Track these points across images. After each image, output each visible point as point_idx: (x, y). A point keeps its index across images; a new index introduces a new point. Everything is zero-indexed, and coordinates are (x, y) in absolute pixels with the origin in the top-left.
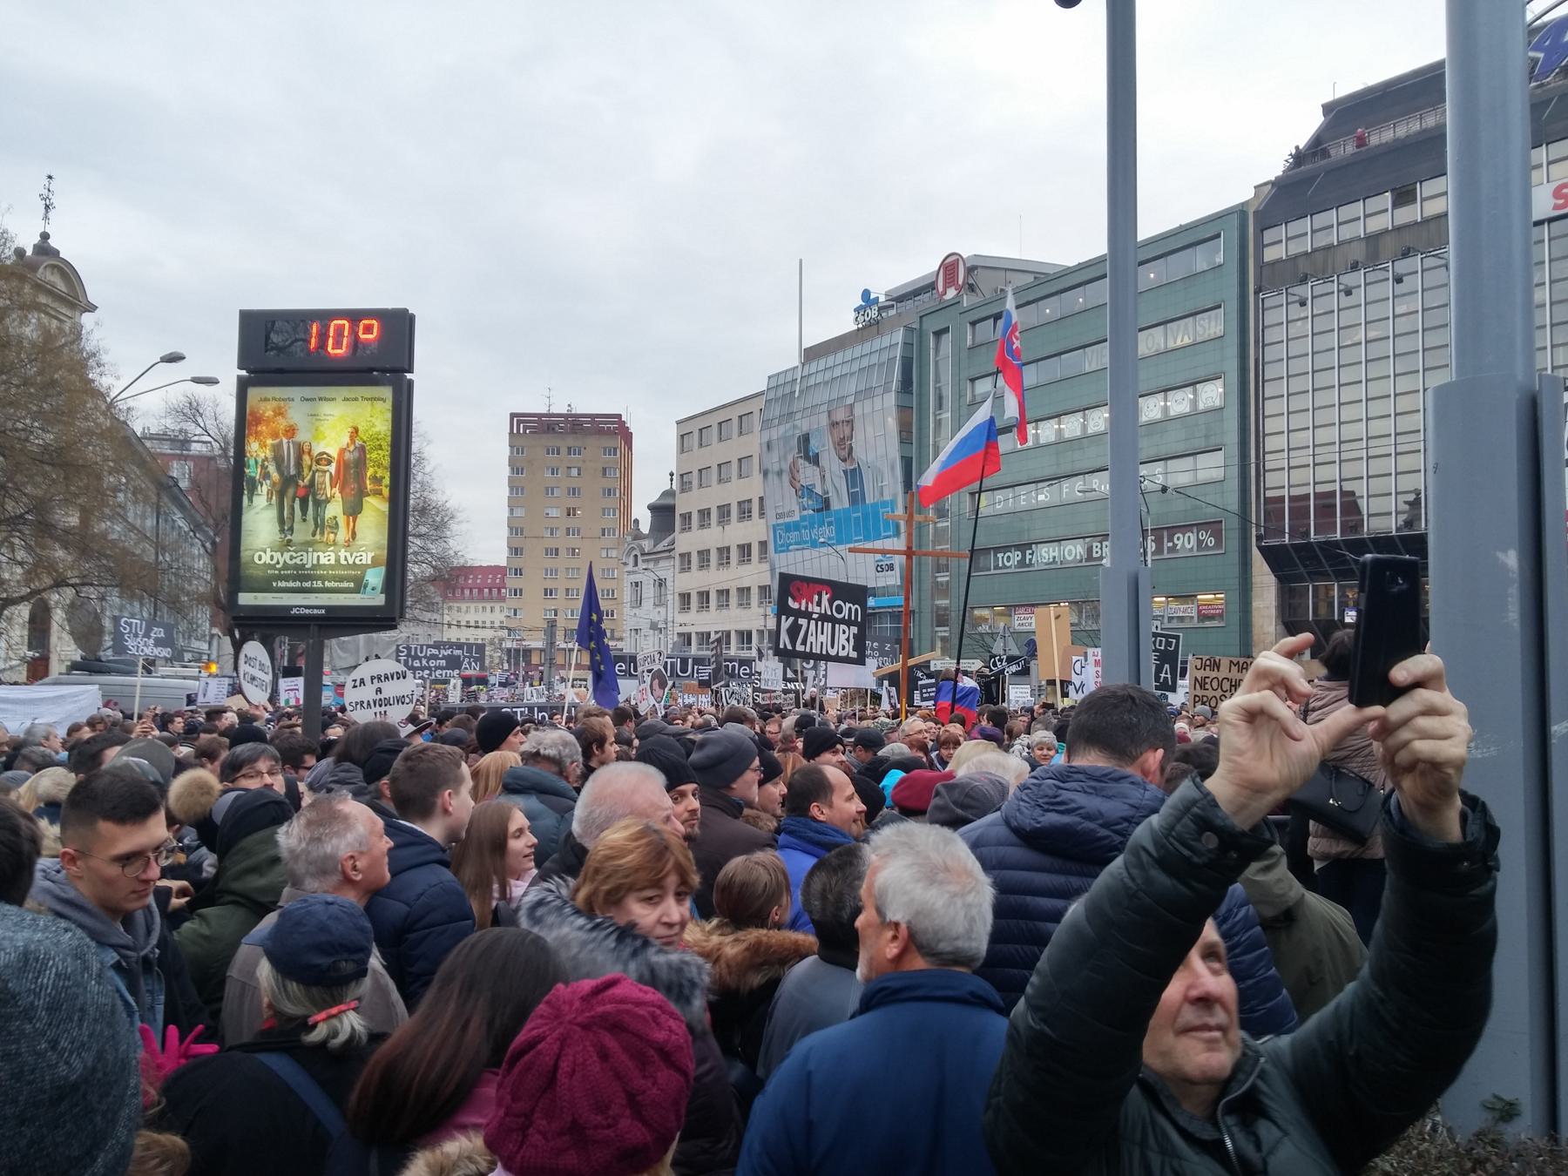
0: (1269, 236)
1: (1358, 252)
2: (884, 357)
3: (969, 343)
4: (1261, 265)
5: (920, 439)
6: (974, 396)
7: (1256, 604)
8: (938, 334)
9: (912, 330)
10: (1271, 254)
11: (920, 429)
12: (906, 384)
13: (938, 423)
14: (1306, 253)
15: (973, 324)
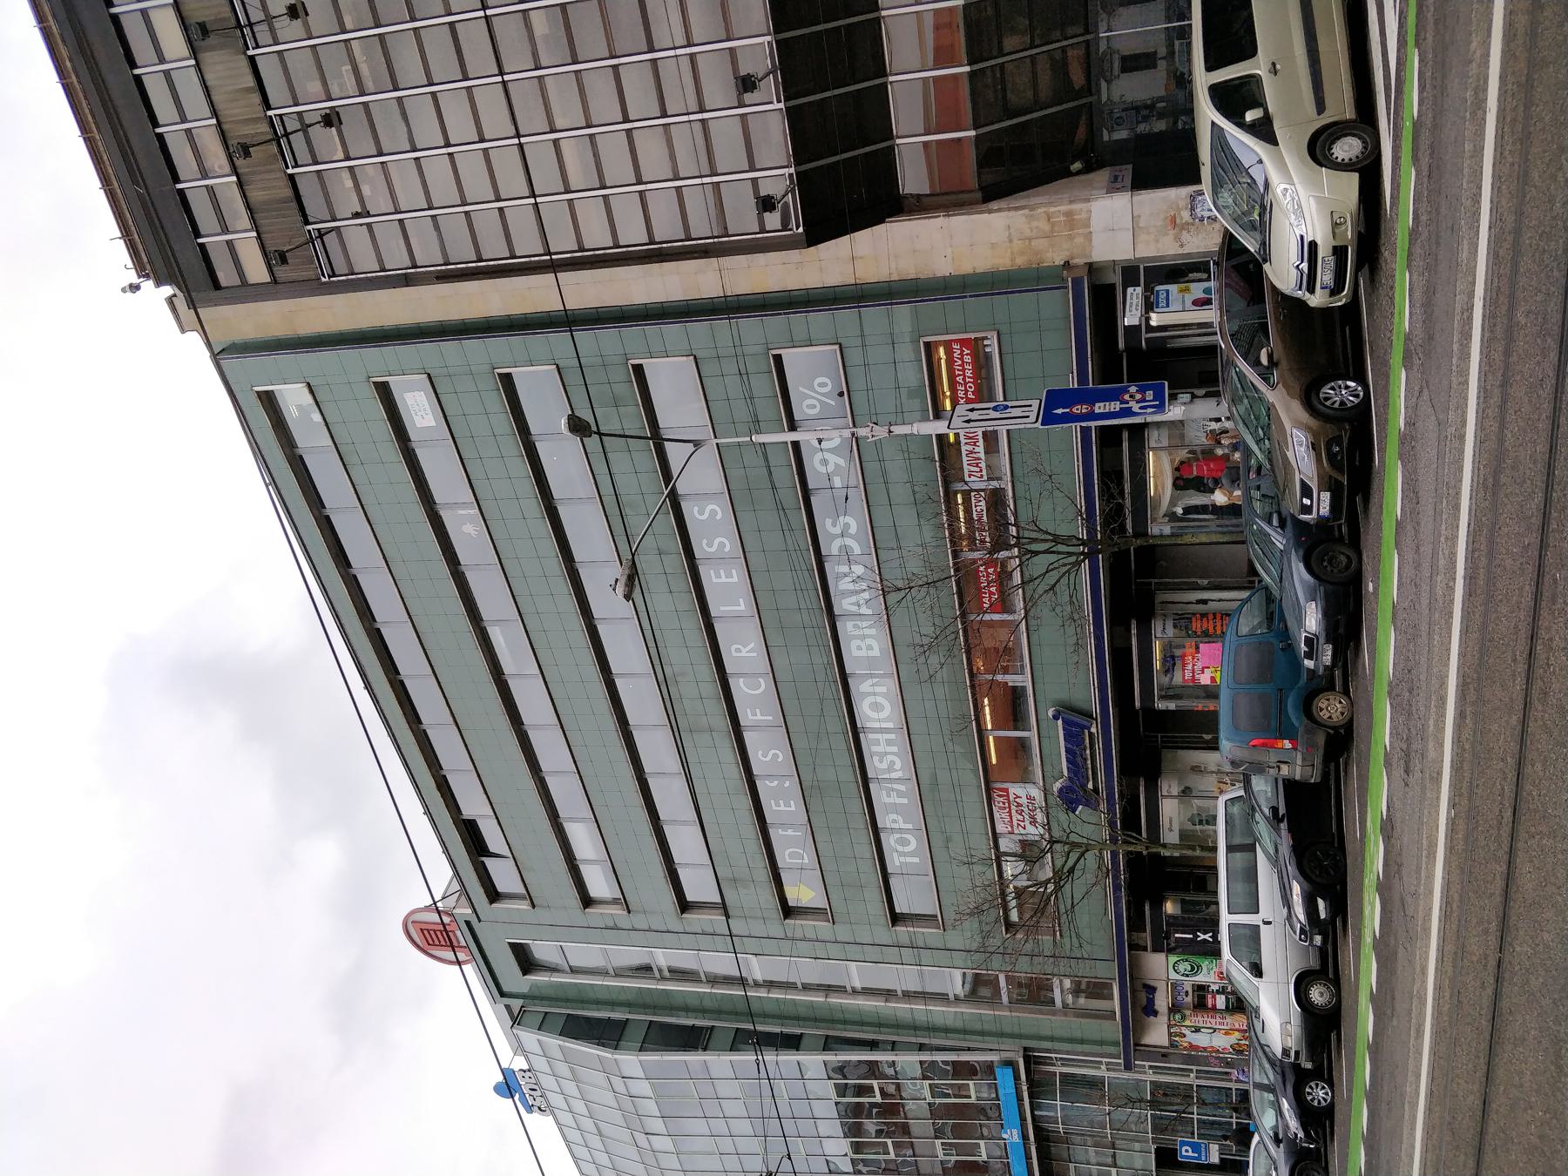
0: (226, 276)
1: (226, 69)
2: (563, 1069)
3: (524, 906)
4: (275, 288)
5: (703, 1011)
6: (615, 901)
7: (943, 266)
8: (526, 961)
9: (522, 1011)
10: (257, 271)
11: (687, 1010)
12: (606, 1033)
13: (678, 974)
14: (240, 184)
15: (494, 895)
